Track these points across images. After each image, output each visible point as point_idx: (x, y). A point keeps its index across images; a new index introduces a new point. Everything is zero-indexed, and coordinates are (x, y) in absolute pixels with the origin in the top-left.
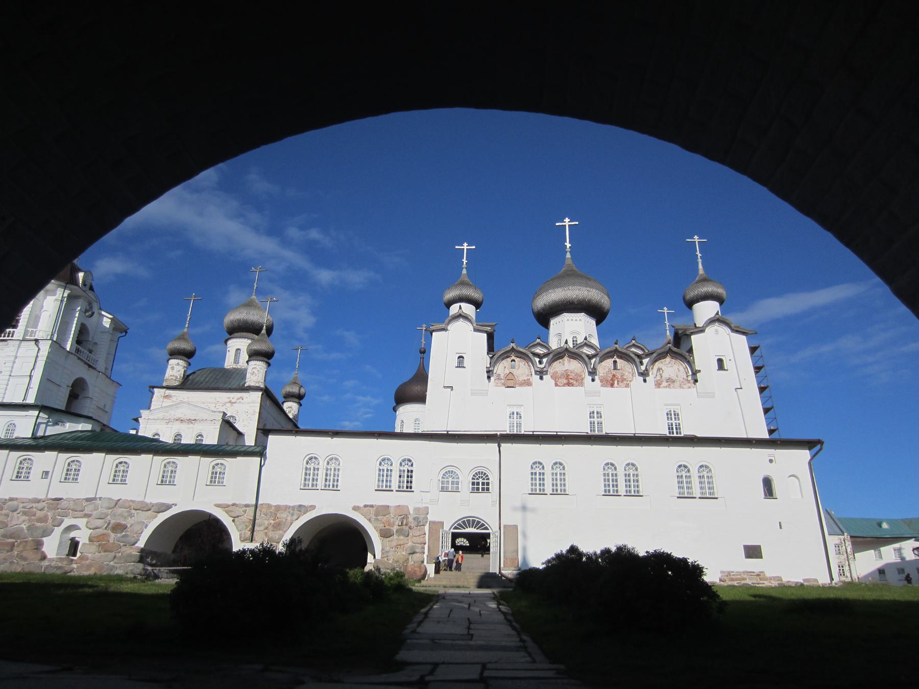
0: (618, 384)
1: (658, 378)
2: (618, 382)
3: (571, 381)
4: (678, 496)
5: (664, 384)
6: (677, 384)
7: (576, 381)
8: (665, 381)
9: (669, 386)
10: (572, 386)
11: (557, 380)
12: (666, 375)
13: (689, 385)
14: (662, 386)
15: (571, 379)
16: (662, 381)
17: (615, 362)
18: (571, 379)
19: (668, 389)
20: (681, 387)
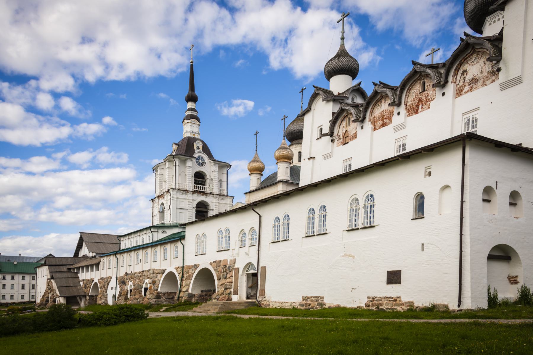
0: (422, 108)
1: (461, 84)
2: (422, 105)
3: (385, 121)
4: (348, 229)
5: (467, 88)
6: (480, 83)
7: (389, 119)
8: (467, 84)
9: (471, 90)
10: (386, 125)
11: (375, 124)
12: (469, 77)
13: (494, 78)
14: (464, 91)
15: (386, 118)
16: (465, 86)
17: (424, 84)
18: (386, 118)
19: (469, 93)
20: (484, 84)
